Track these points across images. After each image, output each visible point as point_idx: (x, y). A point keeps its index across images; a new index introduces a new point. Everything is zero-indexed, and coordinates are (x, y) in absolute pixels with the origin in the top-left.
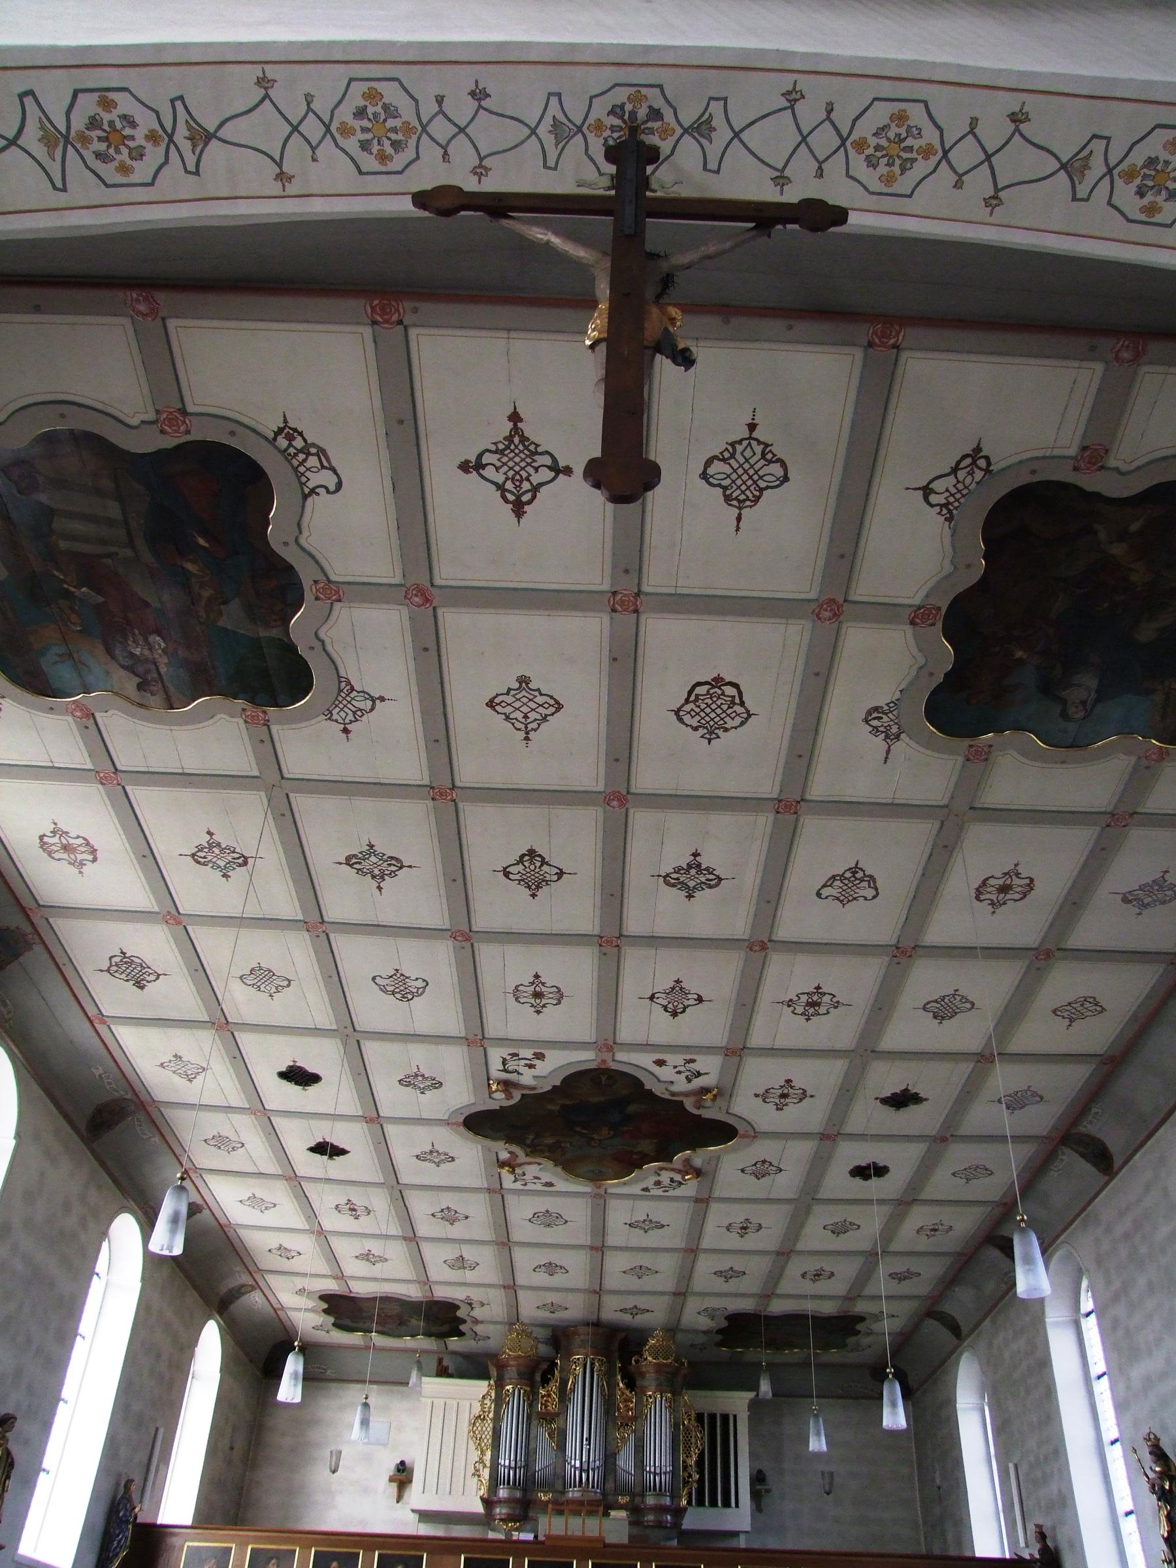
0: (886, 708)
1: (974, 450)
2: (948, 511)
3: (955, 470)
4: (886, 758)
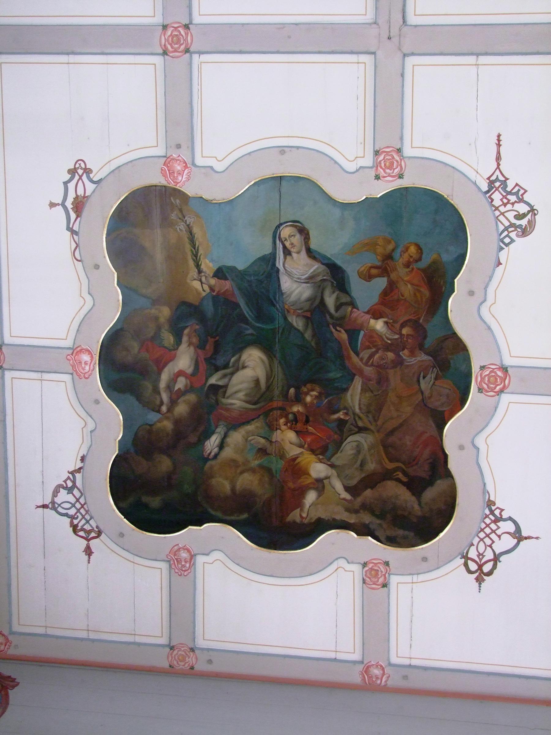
0: (513, 235)
1: (483, 580)
2: (493, 513)
3: (496, 559)
4: (499, 145)
